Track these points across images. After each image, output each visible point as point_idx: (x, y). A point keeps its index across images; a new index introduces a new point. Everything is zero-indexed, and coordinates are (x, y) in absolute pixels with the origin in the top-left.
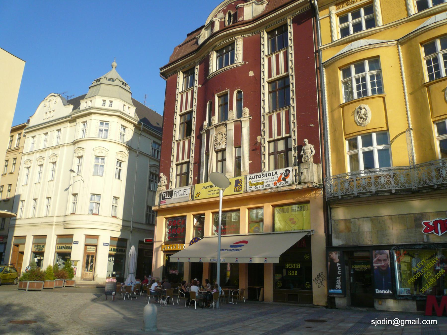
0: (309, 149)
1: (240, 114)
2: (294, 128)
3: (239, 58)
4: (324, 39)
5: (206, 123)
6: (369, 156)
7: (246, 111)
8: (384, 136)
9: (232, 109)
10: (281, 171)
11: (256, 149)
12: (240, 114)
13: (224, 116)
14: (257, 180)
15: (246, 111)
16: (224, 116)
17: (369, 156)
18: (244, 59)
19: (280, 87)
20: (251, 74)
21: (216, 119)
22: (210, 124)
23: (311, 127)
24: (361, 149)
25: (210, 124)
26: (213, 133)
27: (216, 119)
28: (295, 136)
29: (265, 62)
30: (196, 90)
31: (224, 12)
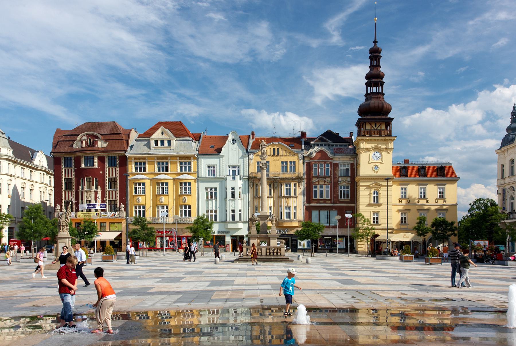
0: (123, 206)
1: (97, 188)
2: (118, 198)
3: (96, 165)
4: (129, 171)
5: (80, 187)
6: (140, 212)
7: (99, 187)
8: (144, 207)
9: (93, 185)
10: (113, 213)
11: (103, 201)
12: (97, 188)
13: (89, 187)
14: (104, 214)
15: (99, 187)
16: (89, 187)
17: (140, 212)
18: (98, 166)
19: (112, 181)
20: (101, 172)
21: (86, 187)
22: (83, 188)
23: (123, 199)
24: (138, 209)
25: (83, 188)
26: (85, 194)
27: (86, 187)
28: (118, 201)
29: (107, 169)
30: (73, 170)
31: (88, 137)
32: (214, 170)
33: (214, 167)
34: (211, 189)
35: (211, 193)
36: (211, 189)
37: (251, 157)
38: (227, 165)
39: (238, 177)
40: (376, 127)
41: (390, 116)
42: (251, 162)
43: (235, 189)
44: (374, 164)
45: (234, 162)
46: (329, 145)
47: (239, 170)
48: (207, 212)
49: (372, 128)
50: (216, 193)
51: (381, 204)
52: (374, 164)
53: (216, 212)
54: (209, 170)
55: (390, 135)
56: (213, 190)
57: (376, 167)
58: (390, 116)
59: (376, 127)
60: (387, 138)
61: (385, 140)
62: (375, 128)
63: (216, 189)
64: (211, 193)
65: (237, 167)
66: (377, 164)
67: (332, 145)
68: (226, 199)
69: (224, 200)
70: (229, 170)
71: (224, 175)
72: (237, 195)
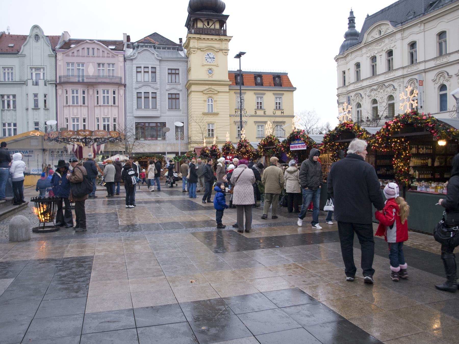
32: (12, 73)
33: (12, 69)
34: (8, 97)
35: (9, 102)
36: (8, 97)
37: (60, 56)
38: (29, 67)
39: (41, 83)
40: (208, 25)
41: (225, 13)
42: (59, 63)
43: (39, 96)
44: (208, 67)
45: (37, 62)
46: (154, 46)
47: (44, 73)
48: (4, 125)
49: (205, 27)
50: (14, 102)
51: (217, 114)
52: (208, 67)
53: (15, 125)
54: (4, 73)
55: (225, 35)
56: (11, 97)
57: (210, 71)
58: (225, 13)
59: (208, 25)
60: (222, 37)
61: (220, 40)
62: (208, 27)
63: (14, 96)
64: (9, 102)
65: (42, 70)
66: (210, 67)
67: (159, 48)
68: (27, 109)
69: (25, 110)
70: (32, 73)
71: (26, 79)
72: (41, 104)
